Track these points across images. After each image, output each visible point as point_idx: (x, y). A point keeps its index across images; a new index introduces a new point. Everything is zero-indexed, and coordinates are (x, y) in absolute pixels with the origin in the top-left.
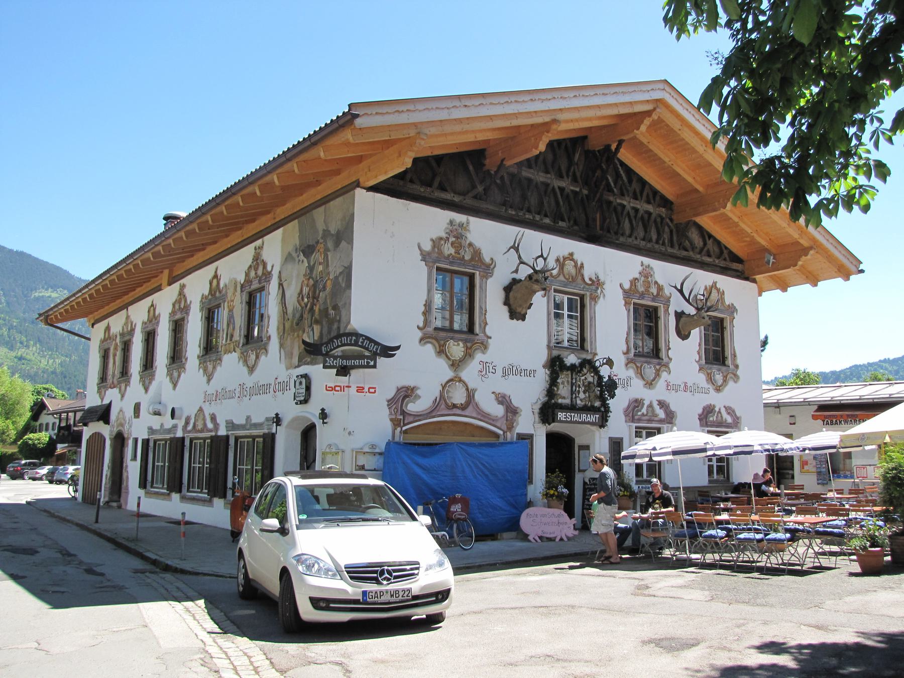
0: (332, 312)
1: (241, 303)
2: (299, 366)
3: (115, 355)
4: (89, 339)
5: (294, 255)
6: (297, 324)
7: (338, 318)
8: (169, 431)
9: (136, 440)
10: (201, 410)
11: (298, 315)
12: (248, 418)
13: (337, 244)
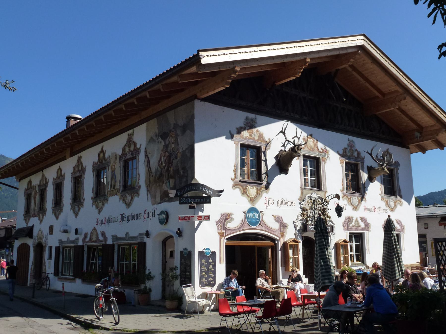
0: (182, 171)
1: (120, 166)
2: (160, 203)
3: (35, 198)
4: (17, 189)
5: (155, 138)
6: (159, 178)
7: (186, 175)
8: (73, 242)
9: (51, 247)
10: (95, 229)
11: (158, 174)
12: (127, 234)
13: (184, 132)
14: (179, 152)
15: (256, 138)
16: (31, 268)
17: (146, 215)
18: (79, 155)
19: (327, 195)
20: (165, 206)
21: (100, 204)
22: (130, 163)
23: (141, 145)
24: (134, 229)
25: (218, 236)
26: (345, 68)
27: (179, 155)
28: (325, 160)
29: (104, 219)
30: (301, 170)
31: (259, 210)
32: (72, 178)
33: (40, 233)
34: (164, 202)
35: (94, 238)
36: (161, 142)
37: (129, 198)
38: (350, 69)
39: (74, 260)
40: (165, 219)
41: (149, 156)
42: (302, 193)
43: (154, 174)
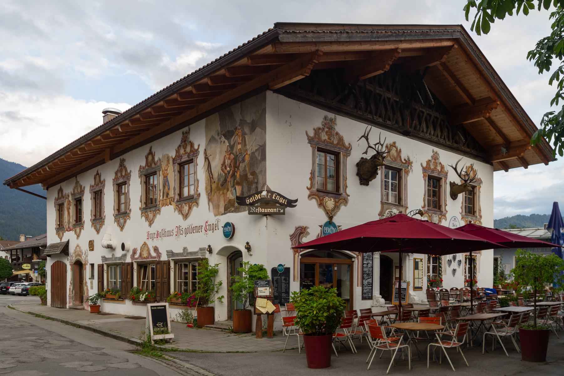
0: (250, 177)
1: (174, 171)
2: (225, 214)
3: (68, 209)
4: (46, 198)
5: (217, 137)
6: (222, 185)
8: (120, 258)
9: (92, 265)
10: (145, 244)
11: (222, 179)
12: (185, 249)
13: (253, 129)
14: (247, 154)
15: (335, 142)
16: (70, 289)
17: (208, 227)
18: (122, 157)
19: (408, 211)
20: (231, 217)
21: (151, 215)
22: (186, 166)
23: (199, 146)
24: (193, 244)
25: (291, 252)
26: (435, 66)
27: (247, 158)
28: (407, 173)
29: (156, 233)
30: (382, 182)
31: (337, 224)
32: (114, 185)
33: (78, 249)
34: (230, 212)
35: (145, 254)
36: (224, 142)
37: (186, 208)
38: (441, 68)
39: (121, 277)
40: (230, 232)
41: (210, 158)
42: (382, 207)
43: (216, 180)
